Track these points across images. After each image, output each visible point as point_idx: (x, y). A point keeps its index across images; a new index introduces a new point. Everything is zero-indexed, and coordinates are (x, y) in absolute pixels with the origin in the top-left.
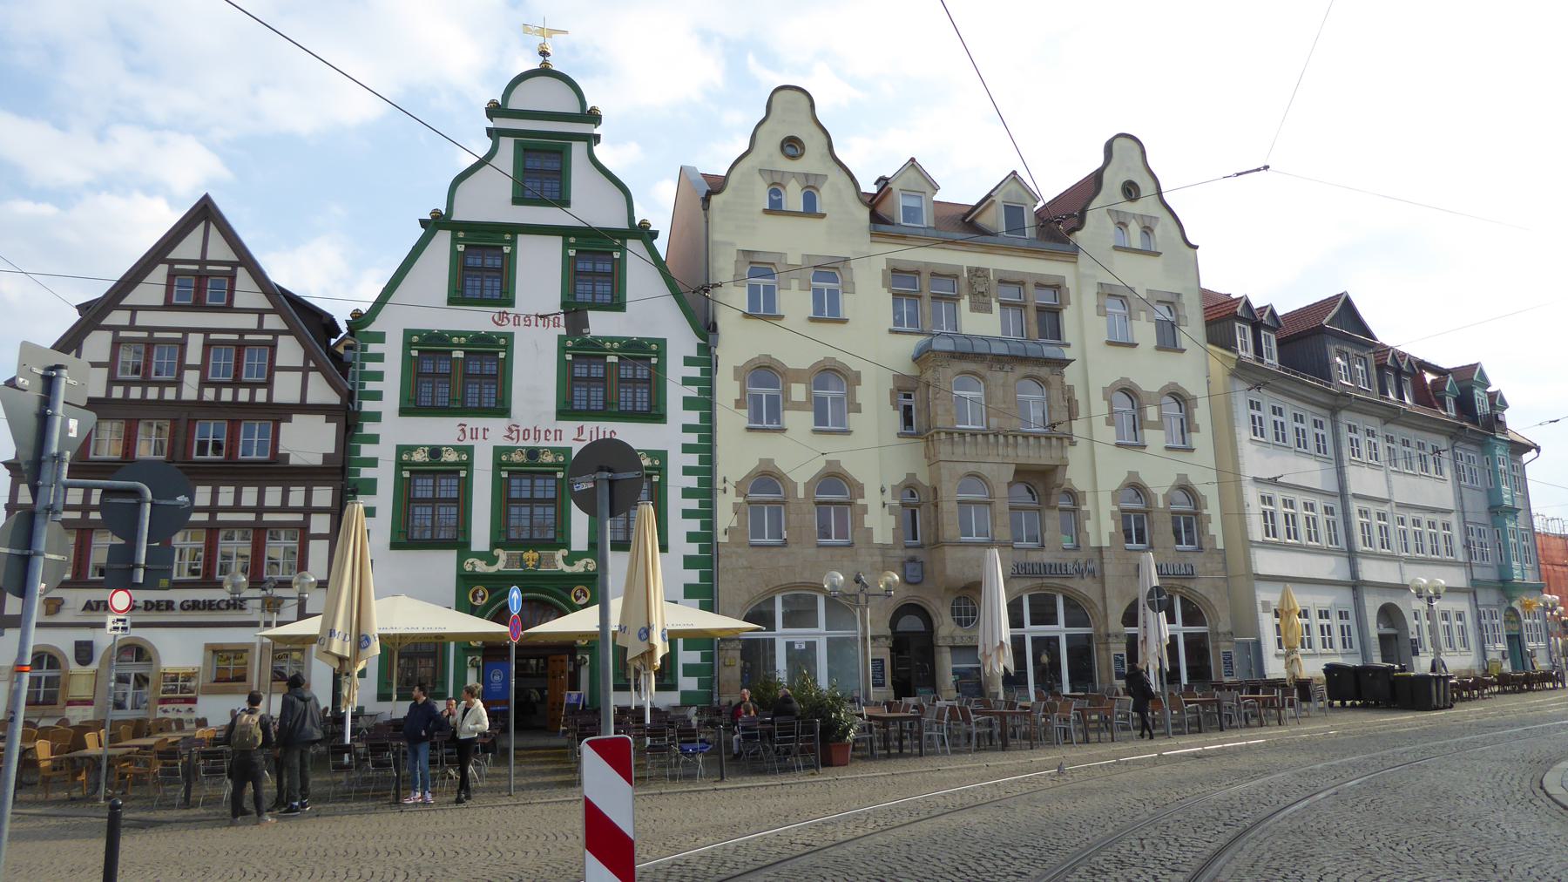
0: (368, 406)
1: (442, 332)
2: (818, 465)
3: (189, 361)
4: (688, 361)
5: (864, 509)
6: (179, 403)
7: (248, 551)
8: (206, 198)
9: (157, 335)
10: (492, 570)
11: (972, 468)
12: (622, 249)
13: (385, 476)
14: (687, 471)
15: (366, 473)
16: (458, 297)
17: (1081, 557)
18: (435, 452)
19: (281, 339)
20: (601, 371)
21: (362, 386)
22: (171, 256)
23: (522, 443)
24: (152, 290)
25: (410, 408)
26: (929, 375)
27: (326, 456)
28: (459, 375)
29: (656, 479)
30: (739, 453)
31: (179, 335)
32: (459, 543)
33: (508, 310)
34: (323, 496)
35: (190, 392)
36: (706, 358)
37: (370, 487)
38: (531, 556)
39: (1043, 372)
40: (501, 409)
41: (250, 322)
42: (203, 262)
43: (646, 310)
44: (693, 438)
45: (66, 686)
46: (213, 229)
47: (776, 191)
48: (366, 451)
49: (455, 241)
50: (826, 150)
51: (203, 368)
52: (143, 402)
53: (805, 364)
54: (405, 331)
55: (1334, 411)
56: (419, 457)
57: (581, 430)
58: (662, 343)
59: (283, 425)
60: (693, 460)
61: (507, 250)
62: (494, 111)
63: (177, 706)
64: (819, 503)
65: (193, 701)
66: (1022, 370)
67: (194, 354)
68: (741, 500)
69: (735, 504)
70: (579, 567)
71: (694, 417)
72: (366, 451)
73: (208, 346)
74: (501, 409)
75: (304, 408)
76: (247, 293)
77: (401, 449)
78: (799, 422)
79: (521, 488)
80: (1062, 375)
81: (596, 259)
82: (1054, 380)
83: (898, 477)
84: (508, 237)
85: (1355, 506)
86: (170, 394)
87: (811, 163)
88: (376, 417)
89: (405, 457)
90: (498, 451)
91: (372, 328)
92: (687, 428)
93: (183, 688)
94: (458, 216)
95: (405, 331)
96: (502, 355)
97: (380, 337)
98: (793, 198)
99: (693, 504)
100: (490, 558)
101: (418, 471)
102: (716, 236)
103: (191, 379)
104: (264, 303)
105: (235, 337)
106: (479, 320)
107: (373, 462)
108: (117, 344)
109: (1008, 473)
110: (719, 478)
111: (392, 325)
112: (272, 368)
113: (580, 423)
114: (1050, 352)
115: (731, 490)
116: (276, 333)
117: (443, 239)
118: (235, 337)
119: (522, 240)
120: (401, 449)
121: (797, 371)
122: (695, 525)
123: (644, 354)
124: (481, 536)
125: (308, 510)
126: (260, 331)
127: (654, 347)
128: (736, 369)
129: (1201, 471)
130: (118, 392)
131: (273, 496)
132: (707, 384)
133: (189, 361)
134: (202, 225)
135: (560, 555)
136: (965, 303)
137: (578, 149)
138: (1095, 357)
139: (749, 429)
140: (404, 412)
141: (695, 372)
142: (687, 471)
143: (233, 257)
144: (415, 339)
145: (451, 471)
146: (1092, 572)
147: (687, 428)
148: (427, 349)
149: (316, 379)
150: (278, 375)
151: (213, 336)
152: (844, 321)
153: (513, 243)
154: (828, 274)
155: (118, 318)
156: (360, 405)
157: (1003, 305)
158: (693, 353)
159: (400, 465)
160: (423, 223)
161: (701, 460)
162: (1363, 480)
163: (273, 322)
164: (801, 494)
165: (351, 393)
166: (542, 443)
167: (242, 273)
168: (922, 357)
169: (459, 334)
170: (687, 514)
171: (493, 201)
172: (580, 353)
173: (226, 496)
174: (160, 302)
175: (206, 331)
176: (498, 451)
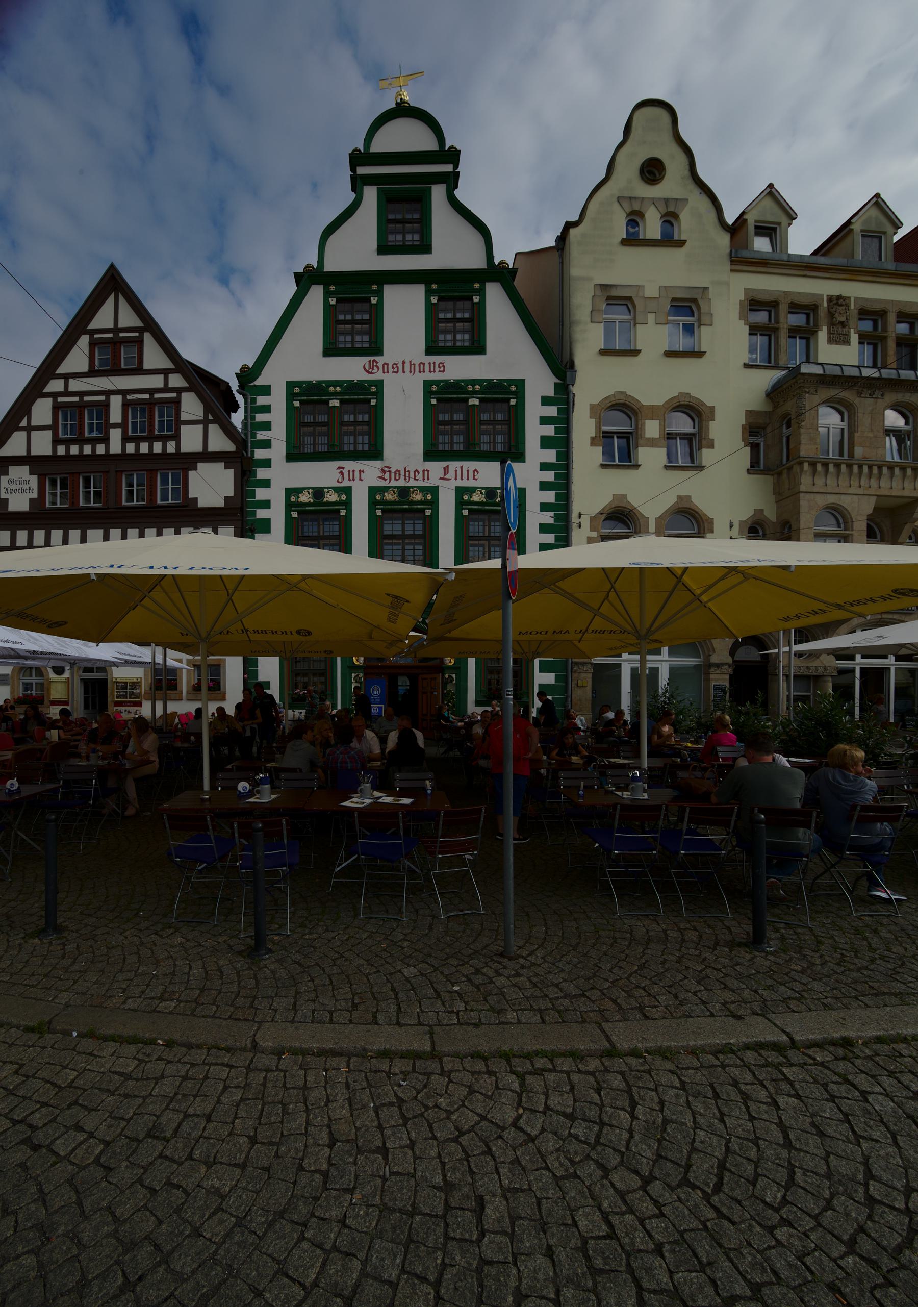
0: (260, 454)
1: (319, 383)
2: (668, 501)
3: (112, 421)
4: (546, 401)
6: (108, 456)
9: (86, 399)
11: (832, 499)
12: (482, 292)
14: (544, 507)
15: (261, 514)
16: (330, 350)
18: (318, 493)
21: (254, 436)
22: (92, 326)
23: (394, 483)
24: (77, 359)
26: (789, 406)
27: (227, 499)
28: (337, 420)
31: (103, 398)
33: (377, 358)
35: (115, 447)
36: (563, 397)
40: (375, 453)
41: (157, 381)
42: (116, 330)
43: (507, 351)
44: (550, 476)
45: (49, 690)
46: (122, 300)
47: (634, 219)
48: (261, 494)
49: (327, 294)
50: (687, 172)
52: (81, 457)
54: (287, 382)
56: (304, 498)
57: (446, 470)
58: (520, 384)
59: (191, 474)
60: (550, 497)
61: (374, 301)
62: (356, 159)
63: (128, 708)
65: (139, 704)
71: (550, 456)
72: (261, 494)
73: (126, 405)
74: (375, 453)
75: (207, 456)
76: (153, 357)
77: (289, 492)
78: (651, 457)
81: (456, 302)
84: (375, 287)
86: (100, 449)
87: (673, 185)
88: (267, 463)
89: (293, 499)
90: (373, 491)
91: (259, 382)
92: (544, 467)
95: (287, 382)
96: (373, 402)
97: (266, 390)
98: (652, 227)
103: (115, 435)
104: (170, 365)
105: (147, 396)
106: (351, 369)
107: (266, 504)
108: (56, 408)
109: (867, 507)
110: (574, 515)
111: (276, 376)
112: (179, 423)
115: (586, 521)
116: (179, 390)
117: (316, 294)
118: (147, 396)
120: (289, 492)
121: (652, 407)
123: (504, 396)
126: (166, 389)
127: (513, 388)
128: (592, 407)
130: (61, 450)
132: (563, 423)
133: (112, 421)
134: (112, 296)
137: (438, 193)
139: (603, 466)
140: (291, 457)
141: (552, 411)
142: (544, 507)
143: (139, 323)
147: (544, 467)
148: (307, 397)
149: (215, 431)
150: (184, 429)
153: (380, 294)
154: (687, 307)
155: (56, 386)
156: (253, 453)
158: (551, 393)
159: (289, 506)
160: (298, 277)
161: (557, 497)
163: (176, 381)
165: (245, 442)
166: (412, 483)
167: (148, 338)
171: (357, 250)
172: (443, 398)
174: (85, 368)
175: (124, 393)
176: (373, 491)
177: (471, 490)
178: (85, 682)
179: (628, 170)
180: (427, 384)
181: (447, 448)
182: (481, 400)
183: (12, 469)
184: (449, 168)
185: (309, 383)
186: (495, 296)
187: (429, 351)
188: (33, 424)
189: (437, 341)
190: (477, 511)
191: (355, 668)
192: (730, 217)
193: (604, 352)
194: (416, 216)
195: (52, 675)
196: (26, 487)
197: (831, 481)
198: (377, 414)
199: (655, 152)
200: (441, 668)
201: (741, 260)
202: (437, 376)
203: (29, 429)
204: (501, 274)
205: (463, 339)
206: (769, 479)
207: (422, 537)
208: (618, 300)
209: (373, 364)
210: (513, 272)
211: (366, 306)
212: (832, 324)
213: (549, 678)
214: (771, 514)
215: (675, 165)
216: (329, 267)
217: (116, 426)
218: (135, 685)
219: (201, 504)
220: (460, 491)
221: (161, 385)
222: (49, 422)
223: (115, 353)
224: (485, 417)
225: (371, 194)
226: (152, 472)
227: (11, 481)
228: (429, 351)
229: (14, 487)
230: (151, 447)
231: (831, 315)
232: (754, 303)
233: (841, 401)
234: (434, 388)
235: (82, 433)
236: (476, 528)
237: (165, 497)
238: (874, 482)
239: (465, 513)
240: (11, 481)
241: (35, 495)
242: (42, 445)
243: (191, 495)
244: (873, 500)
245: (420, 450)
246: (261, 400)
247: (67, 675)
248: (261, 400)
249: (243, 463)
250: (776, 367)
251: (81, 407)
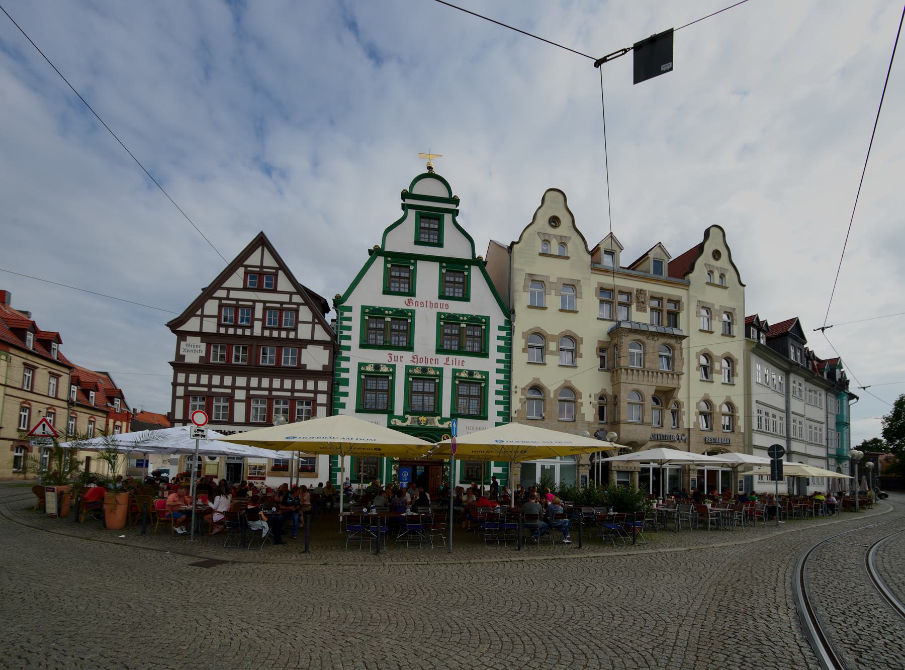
0: (344, 343)
1: (380, 308)
3: (256, 317)
4: (500, 328)
5: (582, 404)
6: (252, 337)
7: (265, 406)
8: (262, 233)
9: (240, 303)
10: (404, 424)
11: (635, 387)
12: (469, 270)
13: (353, 377)
14: (498, 382)
16: (387, 291)
17: (680, 432)
18: (377, 367)
19: (301, 307)
20: (457, 332)
21: (341, 333)
22: (246, 263)
23: (419, 364)
24: (237, 279)
25: (365, 345)
26: (615, 341)
28: (388, 328)
29: (483, 385)
30: (523, 375)
31: (251, 304)
32: (388, 411)
34: (323, 385)
35: (257, 331)
36: (509, 327)
37: (346, 382)
38: (423, 419)
39: (672, 342)
40: (409, 347)
41: (286, 298)
42: (262, 267)
43: (481, 301)
44: (501, 366)
48: (344, 365)
49: (386, 262)
50: (571, 224)
51: (263, 320)
52: (235, 336)
53: (557, 333)
54: (362, 306)
55: (787, 373)
56: (369, 369)
57: (448, 359)
59: (303, 350)
60: (501, 377)
61: (412, 268)
64: (560, 401)
65: (264, 479)
66: (662, 340)
67: (259, 314)
68: (523, 397)
70: (446, 425)
72: (344, 365)
74: (409, 347)
75: (313, 342)
76: (283, 283)
77: (360, 365)
78: (552, 360)
79: (418, 386)
80: (681, 343)
82: (677, 346)
83: (597, 390)
84: (412, 261)
85: (792, 417)
86: (248, 332)
87: (564, 229)
88: (348, 348)
91: (345, 304)
92: (499, 361)
93: (259, 473)
95: (362, 306)
96: (409, 321)
97: (349, 309)
99: (501, 398)
101: (369, 376)
102: (516, 265)
103: (258, 326)
104: (293, 290)
105: (279, 305)
106: (398, 302)
108: (221, 306)
109: (652, 391)
111: (356, 302)
112: (297, 322)
113: (447, 356)
114: (676, 332)
115: (519, 391)
116: (298, 304)
117: (380, 260)
118: (279, 305)
120: (360, 365)
122: (501, 408)
123: (479, 323)
124: (399, 409)
125: (316, 392)
126: (290, 303)
128: (523, 333)
129: (737, 395)
130: (222, 330)
131: (299, 384)
132: (509, 340)
133: (256, 317)
136: (634, 307)
137: (448, 218)
138: (698, 336)
139: (529, 363)
140: (362, 346)
141: (503, 334)
142: (498, 382)
143: (277, 265)
144: (367, 310)
145: (385, 376)
146: (684, 440)
147: (499, 361)
148: (372, 314)
149: (318, 327)
151: (268, 305)
152: (576, 312)
153: (415, 264)
155: (221, 293)
157: (652, 309)
158: (503, 324)
159: (360, 372)
160: (370, 252)
162: (796, 406)
163: (297, 299)
164: (552, 396)
165: (336, 336)
166: (429, 365)
167: (281, 273)
168: (612, 333)
169: (388, 309)
170: (497, 403)
171: (404, 241)
172: (447, 321)
173: (276, 383)
174: (241, 287)
175: (264, 302)
177: (460, 371)
178: (228, 465)
179: (543, 220)
180: (439, 314)
181: (449, 347)
183: (188, 338)
184: (452, 207)
185: (374, 307)
186: (475, 271)
187: (441, 297)
188: (205, 313)
189: (444, 293)
190: (463, 382)
192: (590, 249)
193: (529, 307)
194: (436, 226)
195: (207, 460)
196: (197, 349)
197: (635, 378)
198: (411, 327)
199: (555, 214)
200: (441, 463)
201: (596, 267)
202: (444, 311)
203: (202, 316)
204: (480, 263)
205: (459, 293)
206: (609, 374)
207: (434, 393)
208: (536, 281)
209: (410, 301)
210: (485, 263)
211: (407, 270)
212: (638, 302)
213: (499, 470)
214: (609, 391)
215: (565, 220)
216: (388, 248)
217: (258, 320)
218: (261, 467)
219: (308, 368)
220: (454, 371)
221: (288, 300)
222: (216, 314)
223: (260, 280)
224: (469, 333)
225: (412, 213)
226: (279, 349)
227: (188, 345)
228: (440, 297)
229: (190, 348)
230: (279, 334)
231: (638, 298)
232: (602, 290)
233: (639, 341)
235: (236, 321)
236: (463, 390)
237: (286, 361)
238: (654, 379)
239: (457, 382)
240: (188, 345)
241: (203, 354)
242: (210, 326)
243: (302, 363)
244: (654, 388)
245: (433, 347)
246: (346, 314)
247: (217, 460)
248: (346, 314)
249: (334, 347)
250: (612, 320)
251: (237, 307)
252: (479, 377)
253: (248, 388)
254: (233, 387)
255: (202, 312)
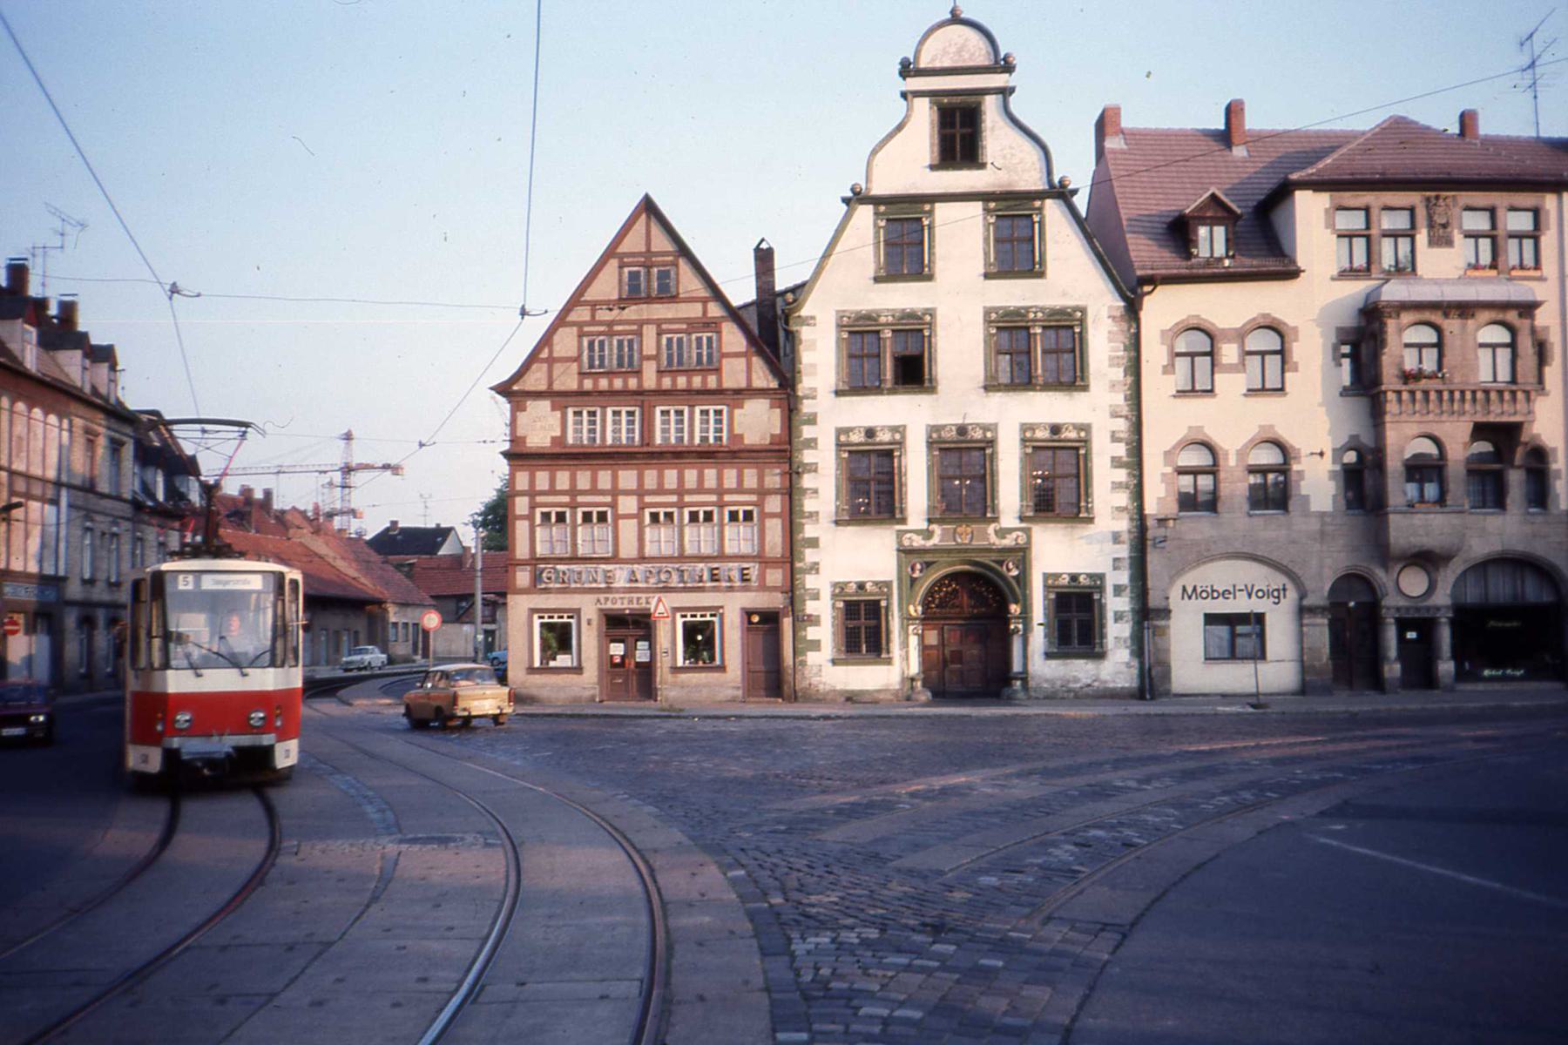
2: (1250, 432)
6: (640, 392)
10: (929, 544)
34: (774, 479)
41: (695, 311)
46: (653, 219)
53: (1237, 323)
69: (1164, 475)
70: (1008, 542)
76: (688, 282)
77: (840, 431)
78: (1231, 385)
89: (843, 438)
94: (877, 190)
100: (928, 534)
106: (902, 297)
119: (940, 208)
120: (840, 431)
135: (991, 529)
149: (757, 362)
155: (581, 314)
163: (715, 310)
164: (1232, 461)
167: (682, 262)
175: (658, 323)
182: (1044, 328)
191: (910, 618)
203: (551, 361)
234: (994, 316)
242: (567, 380)
252: (1073, 435)
253: (640, 492)
254: (615, 492)
255: (551, 352)
